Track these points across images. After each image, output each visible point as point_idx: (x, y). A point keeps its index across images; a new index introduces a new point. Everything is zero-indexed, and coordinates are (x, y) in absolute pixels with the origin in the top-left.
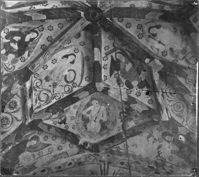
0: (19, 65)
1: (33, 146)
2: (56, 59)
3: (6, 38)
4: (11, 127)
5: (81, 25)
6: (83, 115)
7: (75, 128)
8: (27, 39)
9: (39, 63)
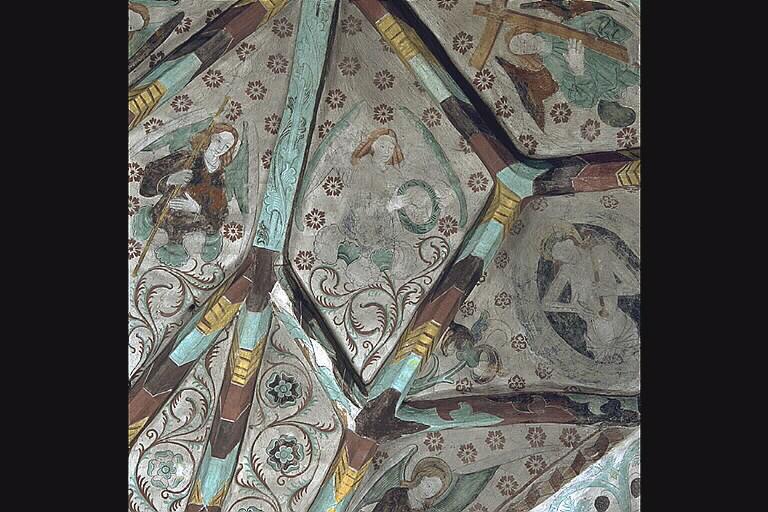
0: (232, 252)
1: (436, 496)
2: (334, 175)
4: (314, 464)
5: (317, 14)
6: (550, 316)
7: (550, 370)
8: (212, 164)
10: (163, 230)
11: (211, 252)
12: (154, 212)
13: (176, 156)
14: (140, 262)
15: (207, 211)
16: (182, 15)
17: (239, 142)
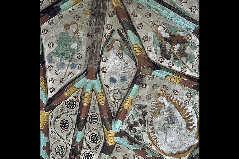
3: (168, 59)
8: (167, 36)
9: (182, 24)
10: (182, 58)
11: (193, 46)
12: (176, 58)
13: (161, 45)
14: (189, 69)
15: (181, 42)
16: (118, 30)
17: (163, 25)
